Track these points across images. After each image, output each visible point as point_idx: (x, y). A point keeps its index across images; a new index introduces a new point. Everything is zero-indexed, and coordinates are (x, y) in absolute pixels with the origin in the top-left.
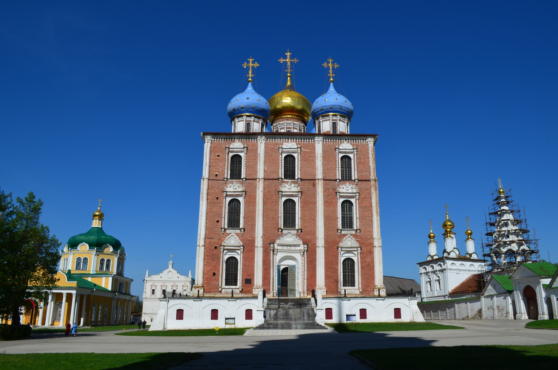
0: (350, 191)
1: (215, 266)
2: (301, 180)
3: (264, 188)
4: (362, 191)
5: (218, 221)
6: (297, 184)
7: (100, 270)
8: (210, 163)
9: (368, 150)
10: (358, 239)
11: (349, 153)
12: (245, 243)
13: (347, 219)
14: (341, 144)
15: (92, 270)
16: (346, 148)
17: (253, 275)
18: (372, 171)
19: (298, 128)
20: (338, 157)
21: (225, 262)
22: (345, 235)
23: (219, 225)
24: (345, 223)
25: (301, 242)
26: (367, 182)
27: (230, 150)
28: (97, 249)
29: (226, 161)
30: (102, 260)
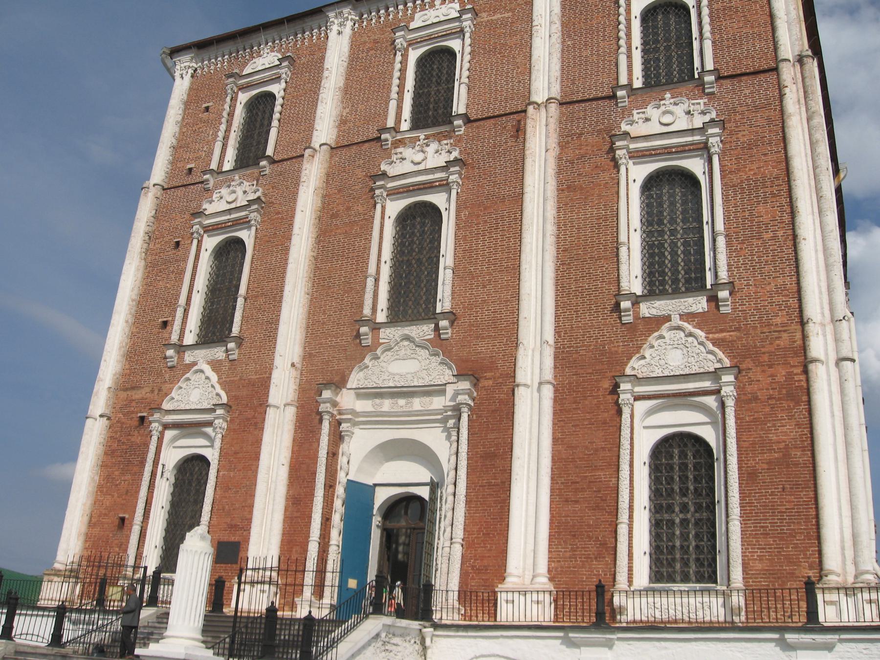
1: (127, 491)
2: (467, 120)
4: (738, 117)
5: (165, 324)
6: (448, 141)
10: (716, 336)
12: (236, 398)
13: (674, 253)
20: (628, 11)
23: (166, 335)
29: (224, 120)
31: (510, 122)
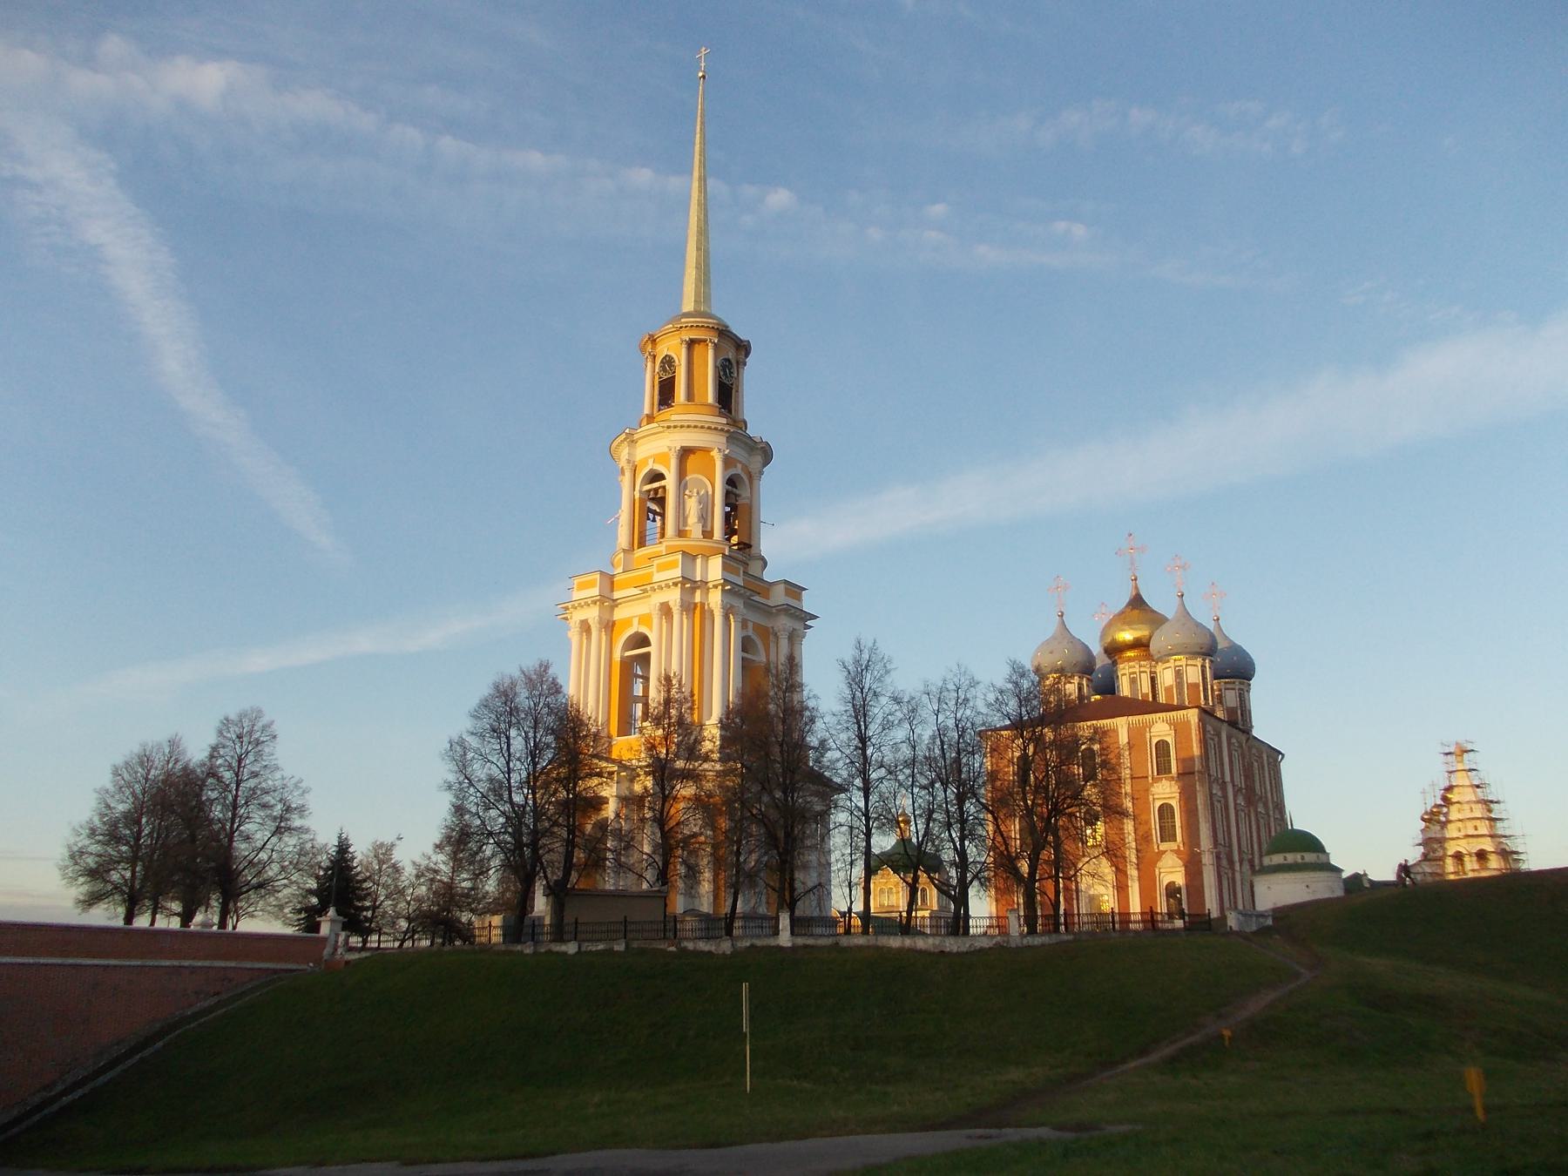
0: (1168, 790)
9: (1191, 729)
11: (1166, 735)
15: (901, 904)
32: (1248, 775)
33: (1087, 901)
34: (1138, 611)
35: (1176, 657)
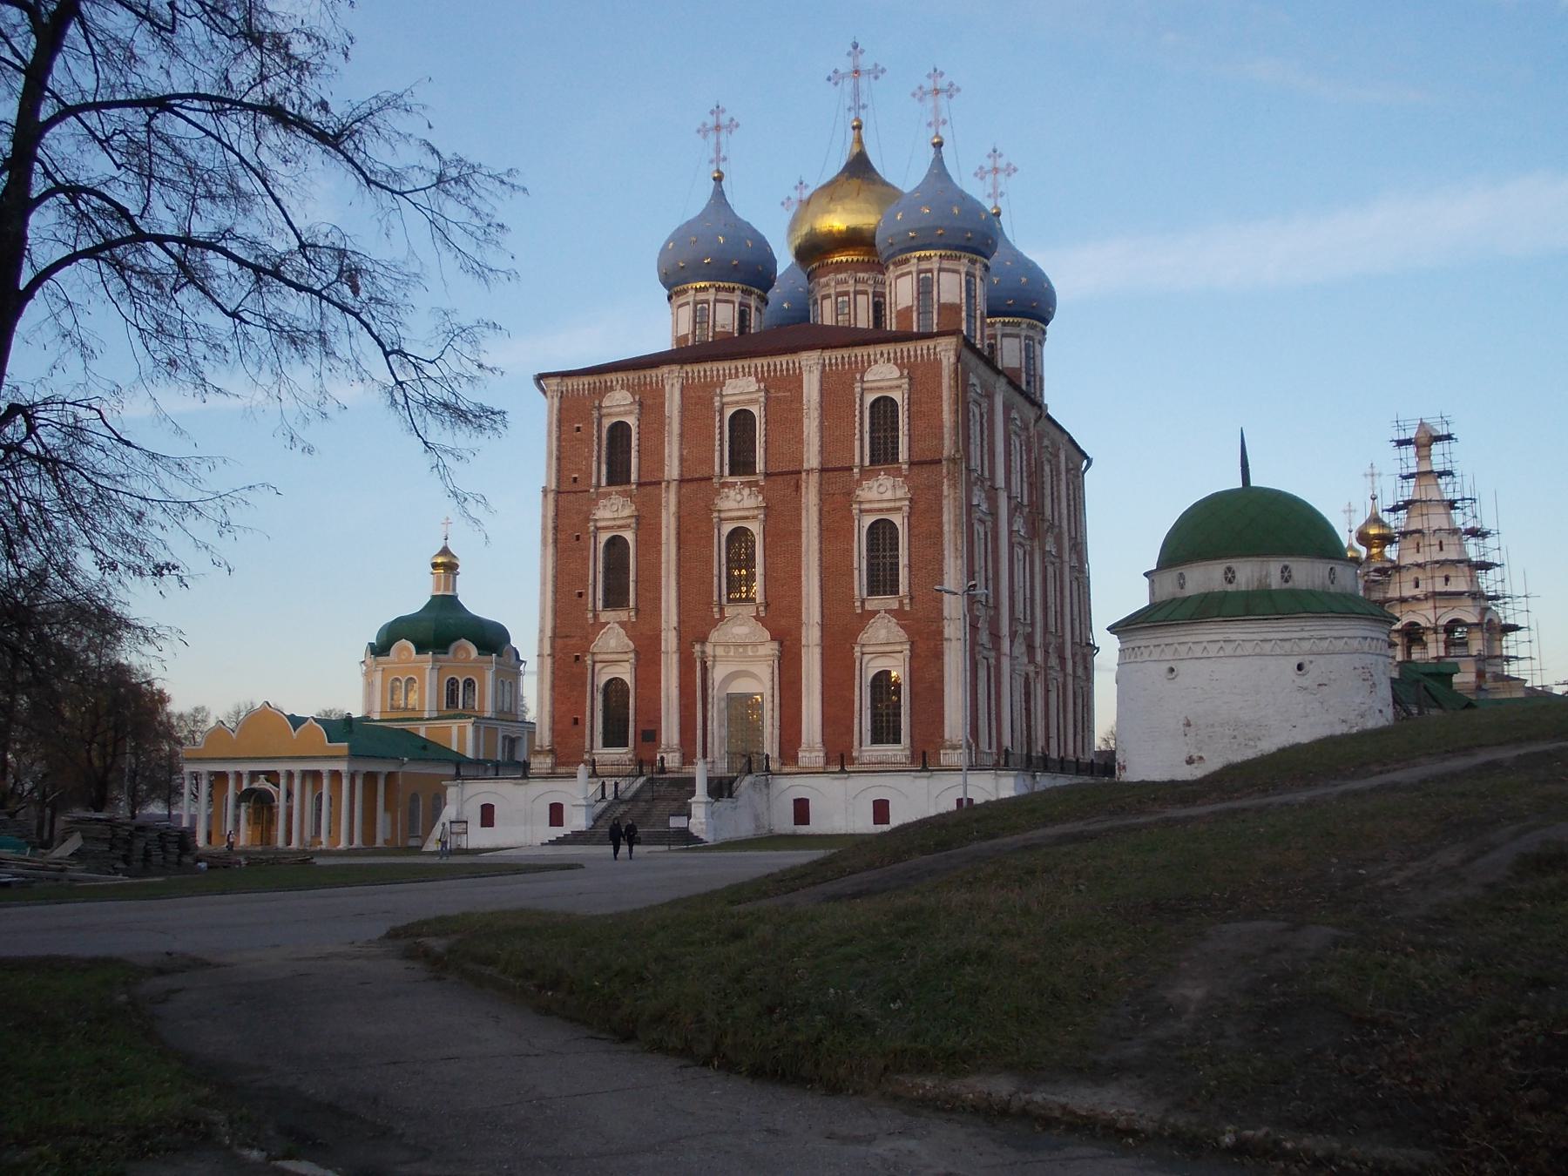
0: (888, 495)
3: (679, 503)
5: (580, 595)
7: (447, 707)
8: (558, 450)
9: (940, 375)
11: (891, 388)
13: (884, 570)
14: (870, 365)
16: (882, 376)
17: (658, 720)
18: (946, 436)
19: (870, 290)
20: (861, 405)
21: (601, 690)
22: (874, 613)
23: (583, 602)
24: (891, 580)
25: (767, 635)
26: (933, 466)
27: (604, 411)
28: (434, 653)
30: (453, 683)
31: (791, 479)
32: (1035, 484)
33: (723, 704)
34: (860, 180)
35: (922, 253)
